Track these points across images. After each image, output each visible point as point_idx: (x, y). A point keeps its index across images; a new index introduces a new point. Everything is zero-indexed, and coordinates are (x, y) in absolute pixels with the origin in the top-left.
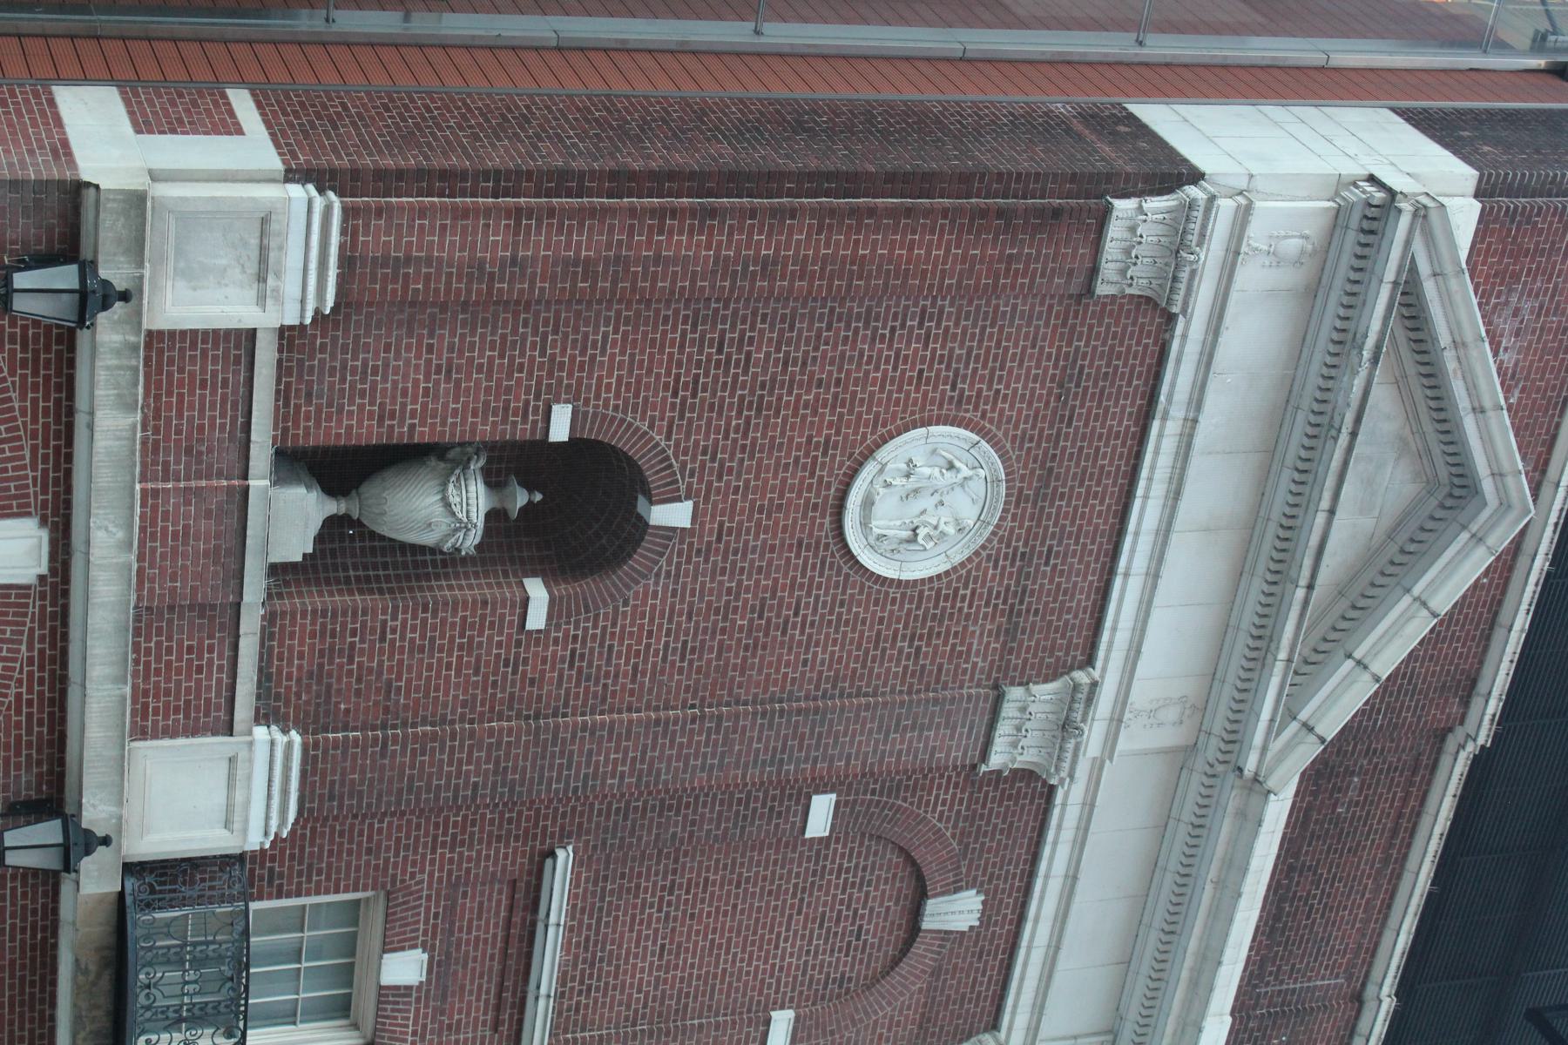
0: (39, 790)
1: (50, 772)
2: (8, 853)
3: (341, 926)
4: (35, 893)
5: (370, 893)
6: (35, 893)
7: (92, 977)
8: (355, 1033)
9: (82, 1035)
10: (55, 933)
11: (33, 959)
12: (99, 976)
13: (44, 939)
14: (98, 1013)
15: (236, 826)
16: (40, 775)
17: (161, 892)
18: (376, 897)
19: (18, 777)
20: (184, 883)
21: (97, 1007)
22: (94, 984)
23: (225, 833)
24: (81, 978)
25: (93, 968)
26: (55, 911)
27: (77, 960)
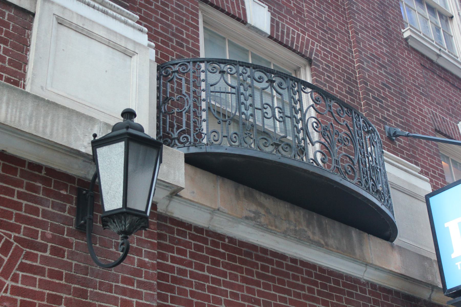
0: (67, 199)
1: (46, 181)
2: (130, 205)
3: (225, 44)
4: (179, 242)
5: (200, 14)
6: (179, 242)
7: (262, 211)
8: (302, 70)
9: (310, 234)
10: (221, 237)
11: (242, 262)
12: (261, 205)
13: (225, 247)
14: (292, 216)
15: (130, 47)
16: (47, 192)
17: (188, 125)
18: (203, 11)
19: (45, 214)
20: (182, 107)
21: (287, 215)
22: (268, 211)
23: (135, 58)
24: (262, 220)
25: (254, 207)
26: (200, 230)
27: (247, 218)
